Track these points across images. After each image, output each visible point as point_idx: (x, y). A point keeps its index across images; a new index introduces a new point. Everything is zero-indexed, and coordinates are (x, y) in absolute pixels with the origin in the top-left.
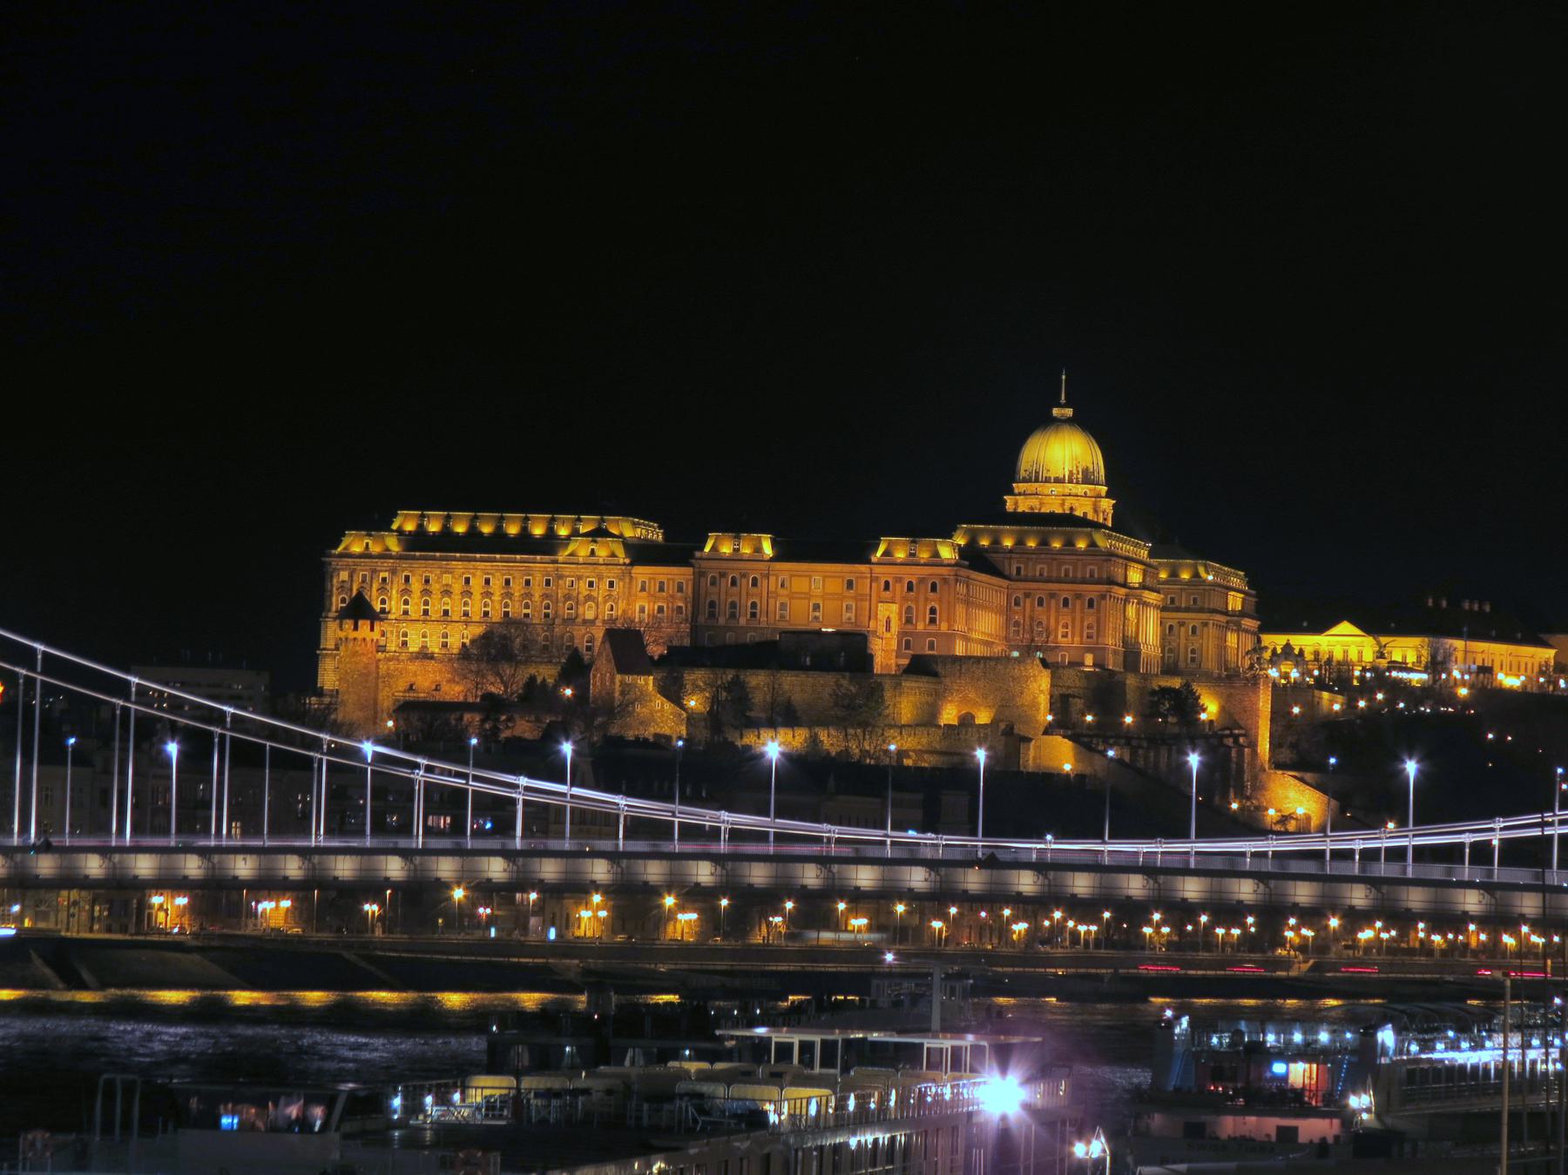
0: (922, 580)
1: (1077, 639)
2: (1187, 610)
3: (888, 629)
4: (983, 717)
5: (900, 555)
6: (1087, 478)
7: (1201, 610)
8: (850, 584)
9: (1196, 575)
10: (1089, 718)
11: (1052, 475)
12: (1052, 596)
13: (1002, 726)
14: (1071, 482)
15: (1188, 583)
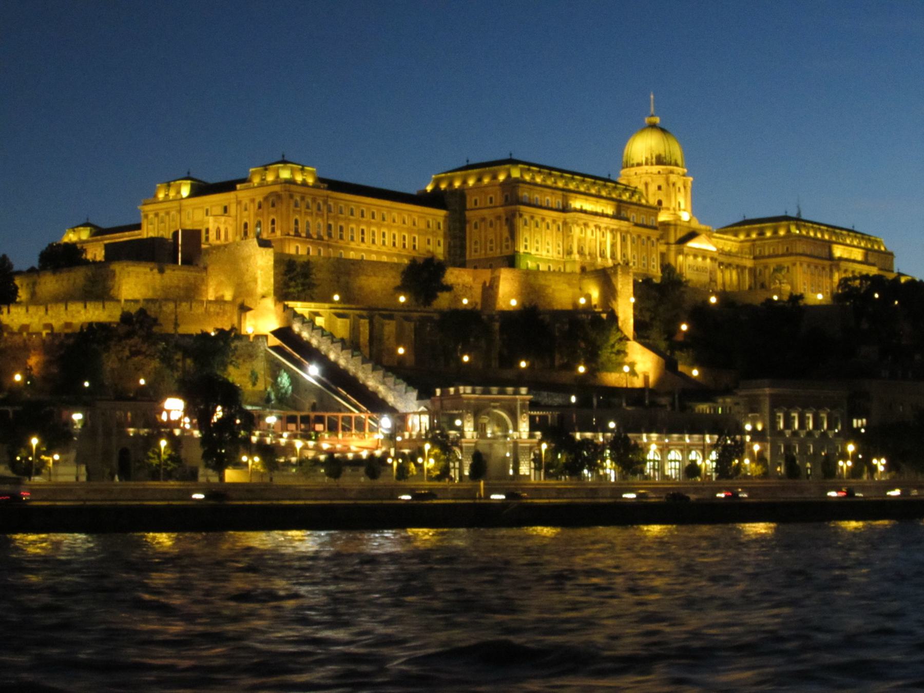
0: (266, 199)
1: (499, 250)
2: (783, 255)
3: (218, 236)
4: (228, 296)
5: (256, 180)
6: (660, 161)
7: (791, 254)
8: (226, 209)
9: (789, 231)
10: (402, 299)
11: (635, 162)
12: (483, 219)
13: (239, 300)
14: (647, 164)
15: (784, 237)
